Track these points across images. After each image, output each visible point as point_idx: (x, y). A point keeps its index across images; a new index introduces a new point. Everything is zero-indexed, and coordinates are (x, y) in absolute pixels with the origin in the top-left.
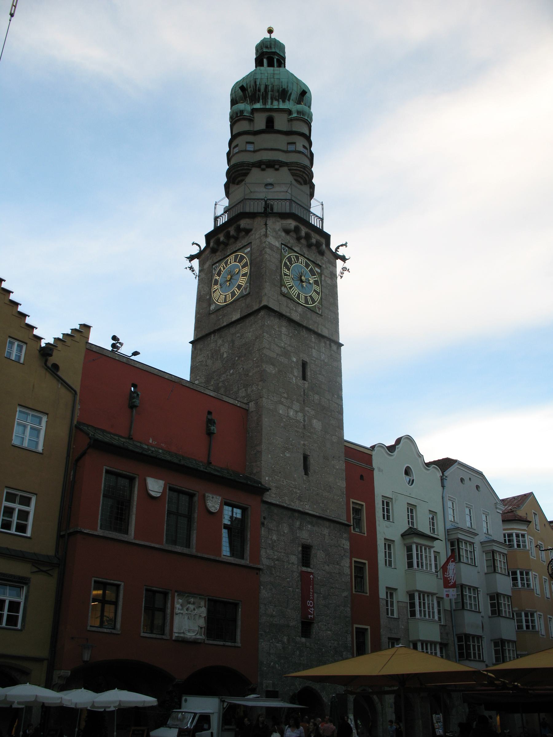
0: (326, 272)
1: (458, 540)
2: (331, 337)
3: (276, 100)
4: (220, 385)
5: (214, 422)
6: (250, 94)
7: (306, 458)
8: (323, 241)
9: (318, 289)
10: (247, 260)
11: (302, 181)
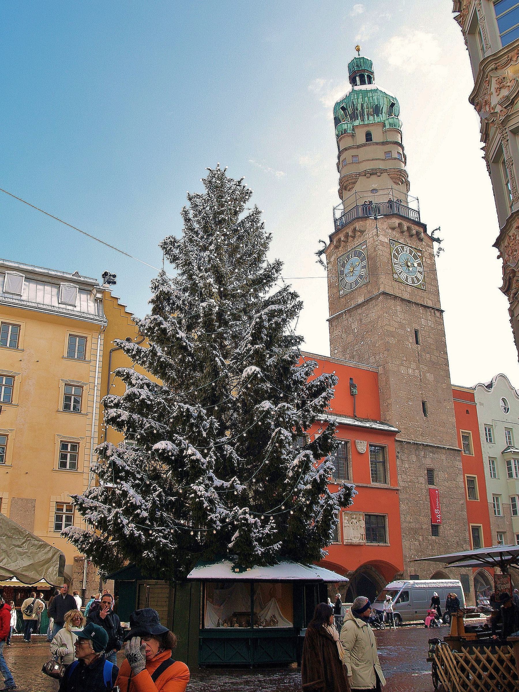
0: (426, 254)
8: (421, 230)
9: (421, 269)
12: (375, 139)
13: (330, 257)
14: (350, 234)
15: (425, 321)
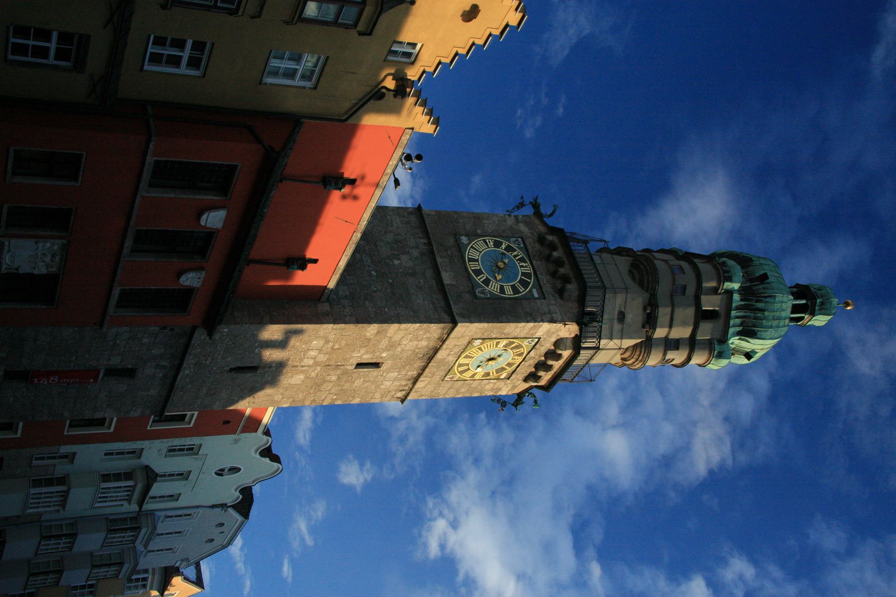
1: (138, 529)
6: (754, 288)
13: (526, 223)
14: (562, 271)
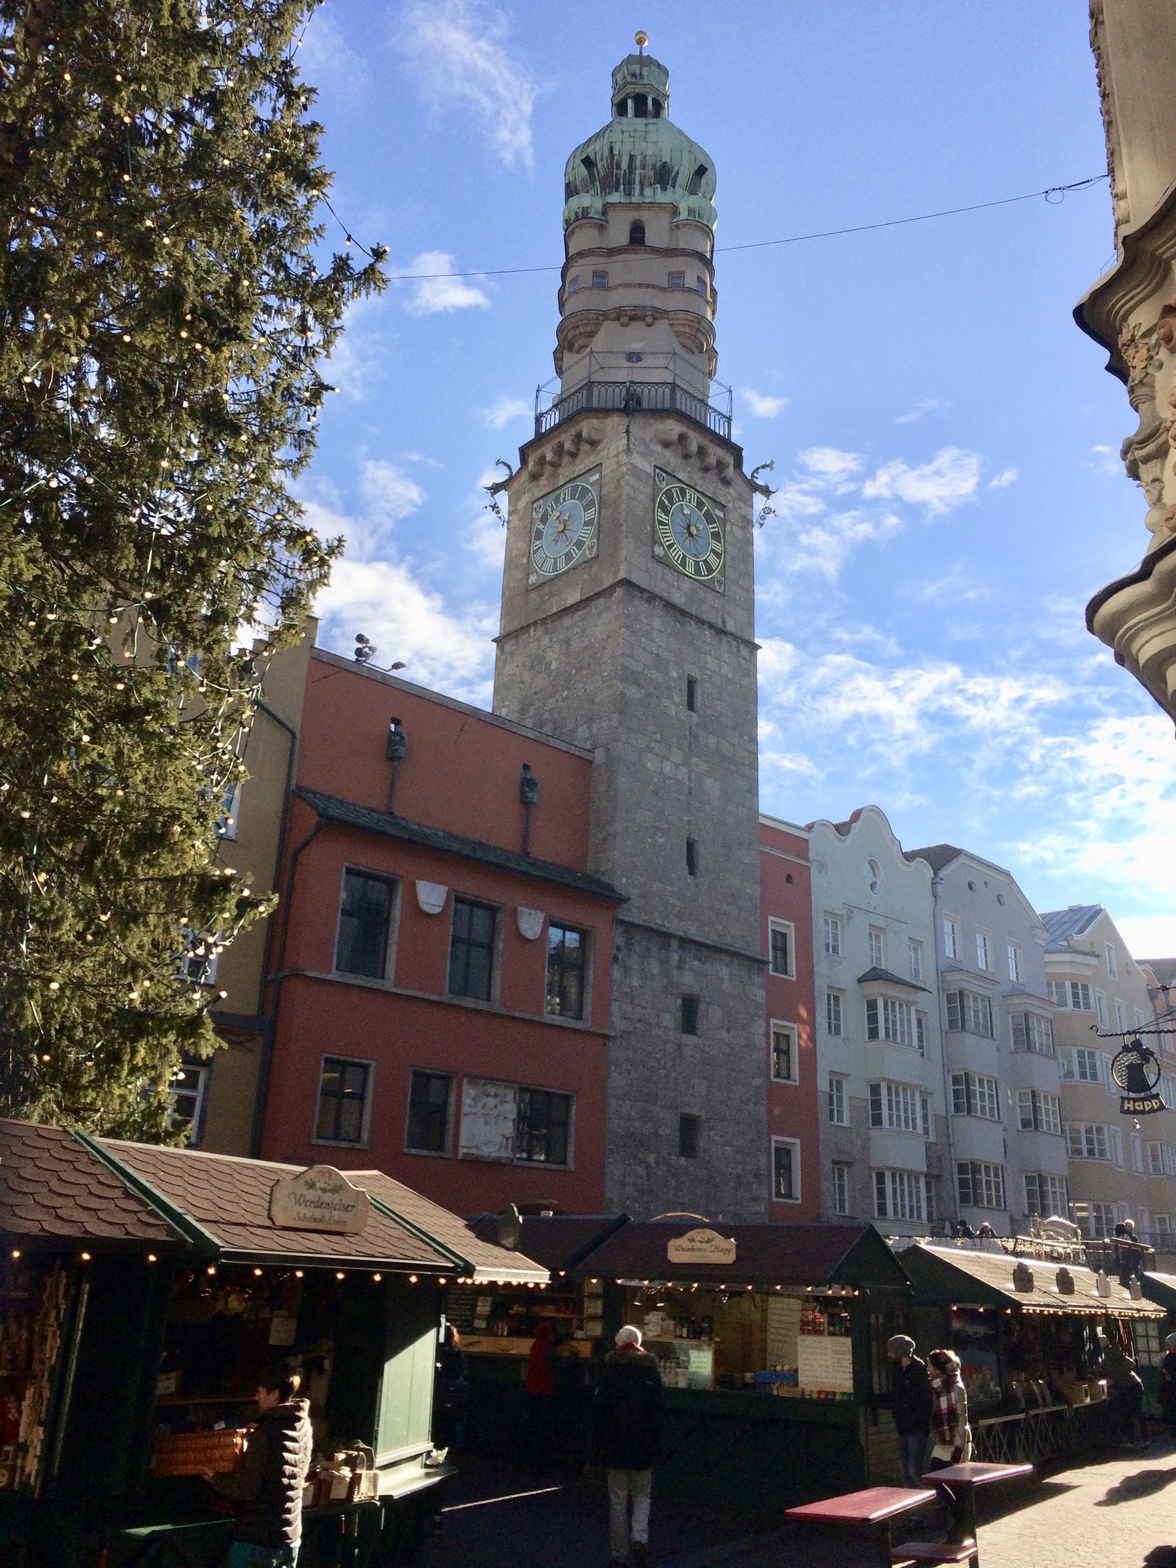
0: (734, 517)
2: (740, 634)
3: (651, 185)
4: (546, 716)
5: (535, 784)
7: (691, 846)
8: (729, 459)
10: (593, 494)
11: (694, 347)
12: (651, 239)
14: (568, 446)
15: (714, 661)
